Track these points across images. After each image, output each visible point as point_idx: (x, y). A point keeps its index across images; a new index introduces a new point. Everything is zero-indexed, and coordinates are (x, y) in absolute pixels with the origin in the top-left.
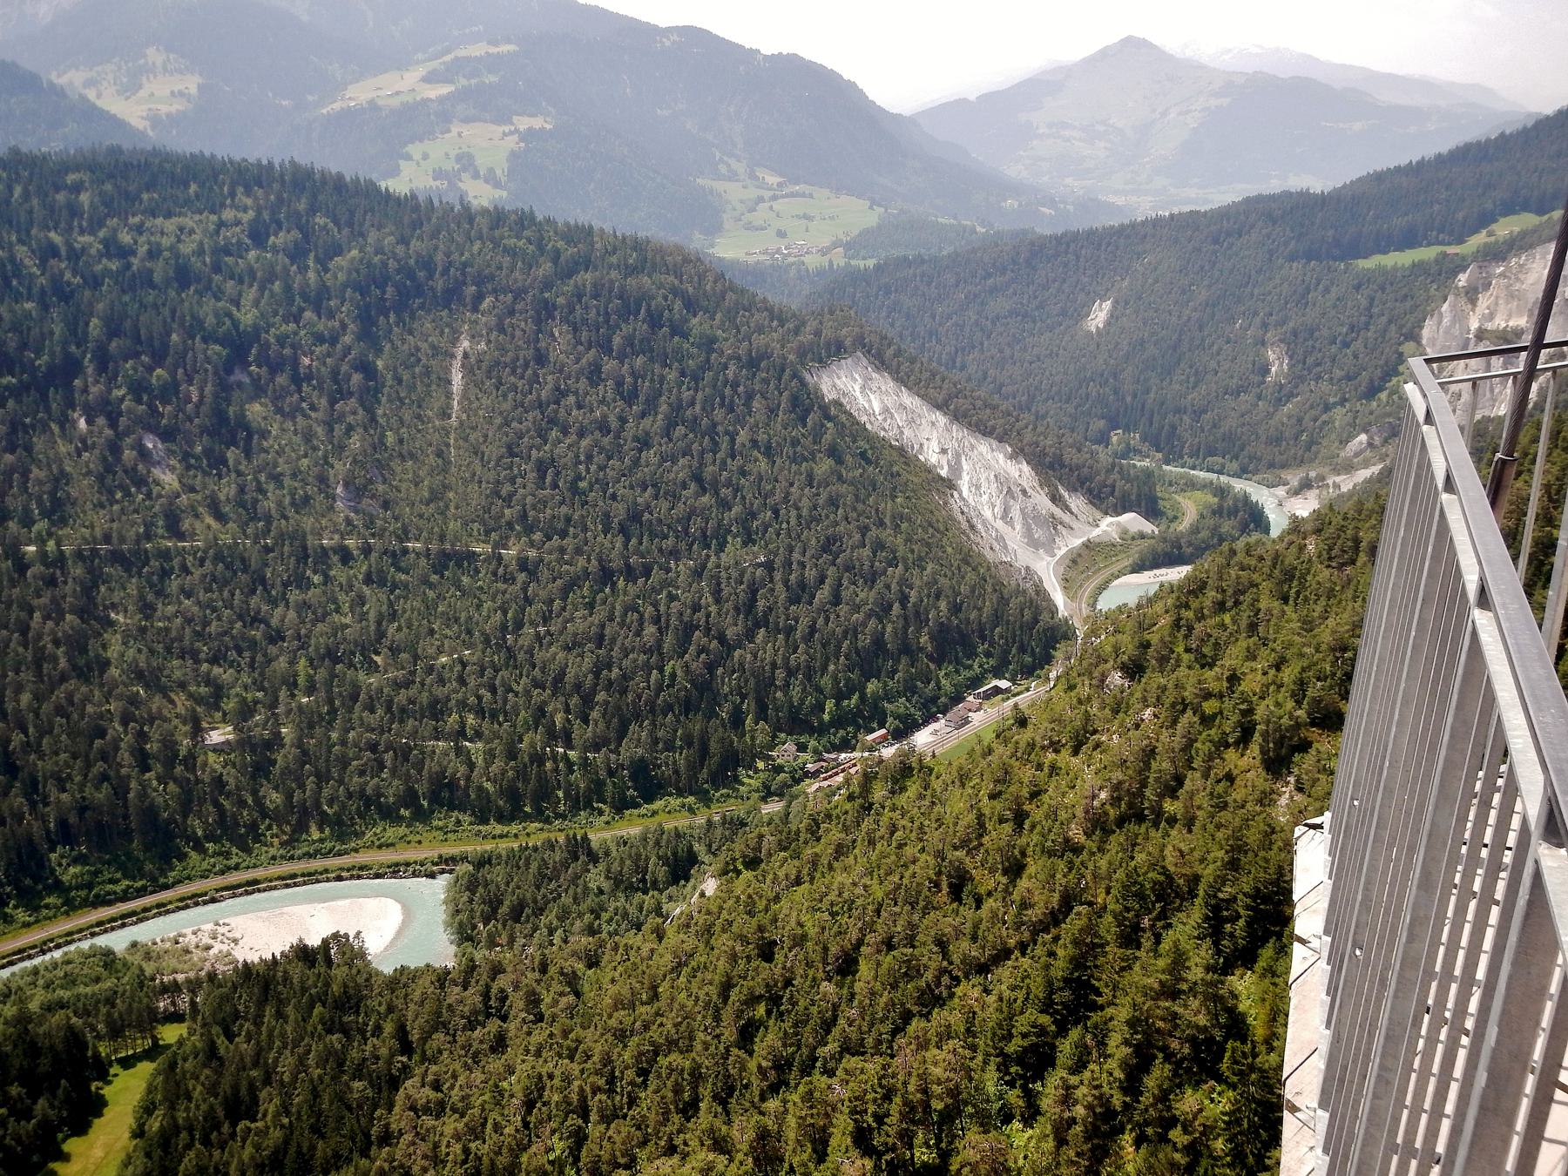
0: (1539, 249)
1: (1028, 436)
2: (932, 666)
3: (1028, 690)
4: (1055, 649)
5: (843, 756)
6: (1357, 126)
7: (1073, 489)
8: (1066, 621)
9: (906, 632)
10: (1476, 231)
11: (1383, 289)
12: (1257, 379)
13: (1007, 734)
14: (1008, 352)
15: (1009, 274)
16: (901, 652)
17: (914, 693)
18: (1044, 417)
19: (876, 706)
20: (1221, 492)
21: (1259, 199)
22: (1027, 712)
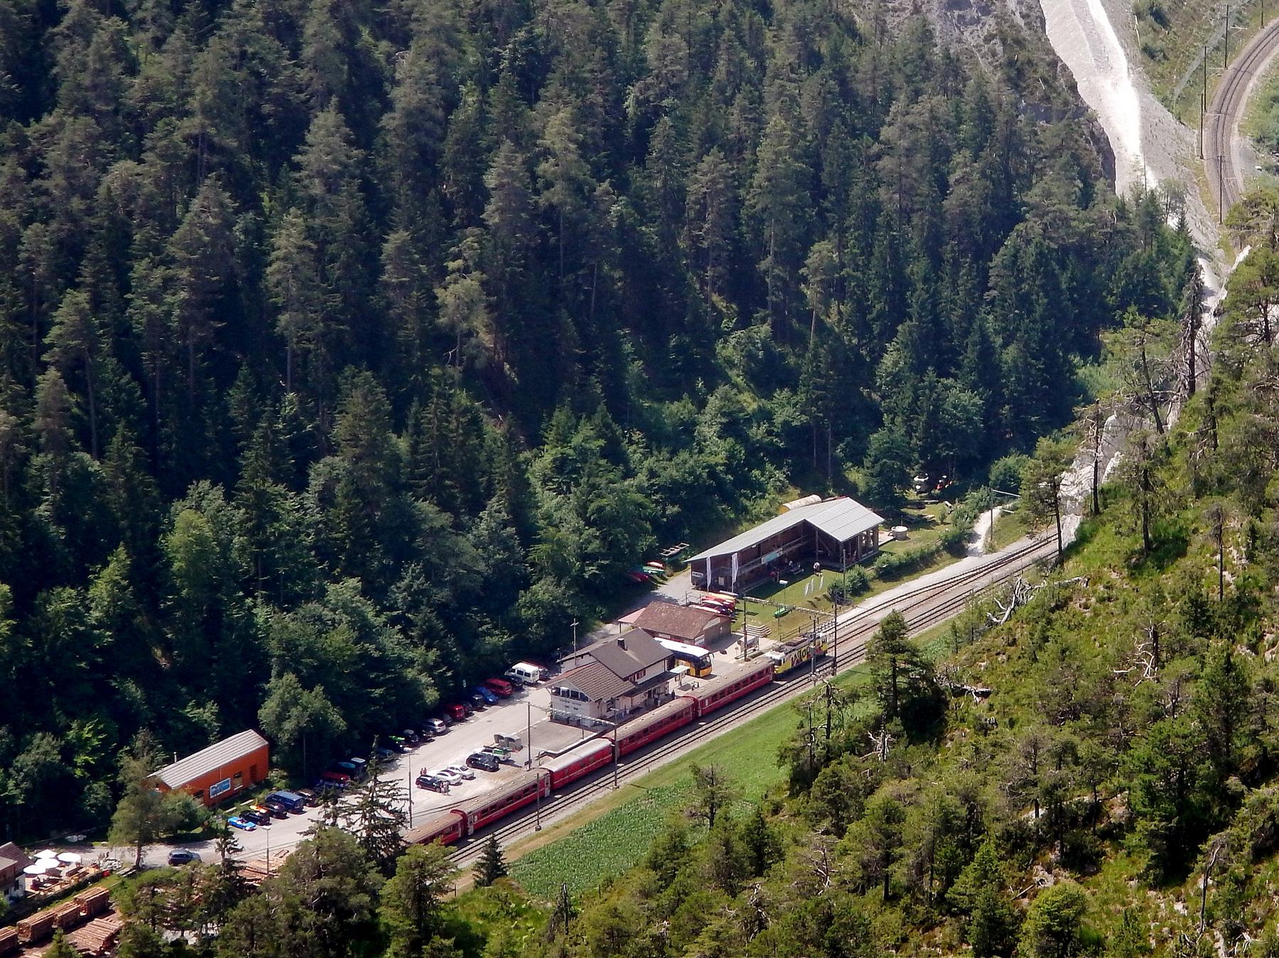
2: (495, 429)
3: (957, 547)
4: (1093, 352)
5: (45, 860)
8: (1151, 213)
9: (371, 261)
13: (848, 769)
16: (341, 355)
17: (404, 554)
19: (214, 623)
22: (945, 664)
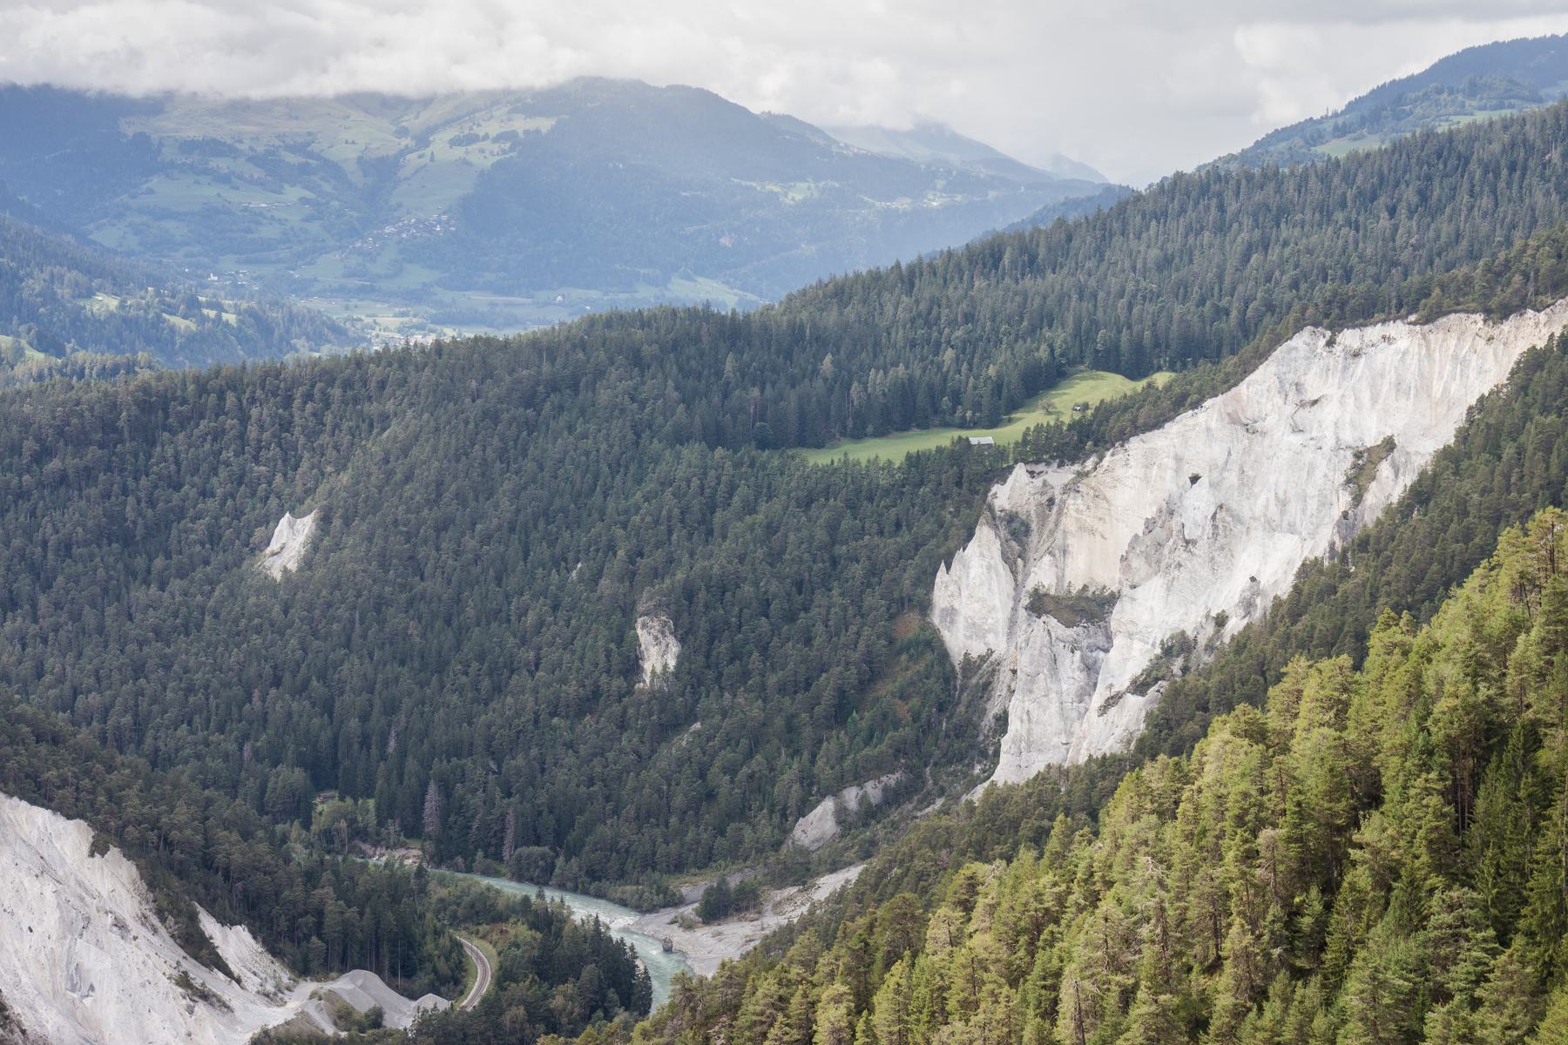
0: (1135, 444)
1: (133, 803)
6: (798, 193)
7: (225, 920)
10: (1015, 405)
11: (852, 506)
12: (618, 683)
14: (90, 617)
15: (93, 452)
18: (170, 761)
20: (548, 923)
21: (615, 320)
